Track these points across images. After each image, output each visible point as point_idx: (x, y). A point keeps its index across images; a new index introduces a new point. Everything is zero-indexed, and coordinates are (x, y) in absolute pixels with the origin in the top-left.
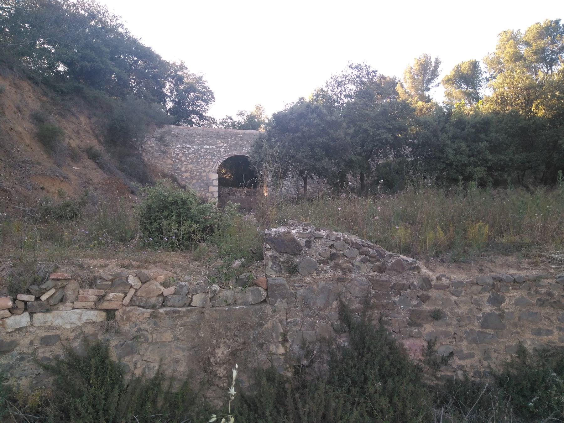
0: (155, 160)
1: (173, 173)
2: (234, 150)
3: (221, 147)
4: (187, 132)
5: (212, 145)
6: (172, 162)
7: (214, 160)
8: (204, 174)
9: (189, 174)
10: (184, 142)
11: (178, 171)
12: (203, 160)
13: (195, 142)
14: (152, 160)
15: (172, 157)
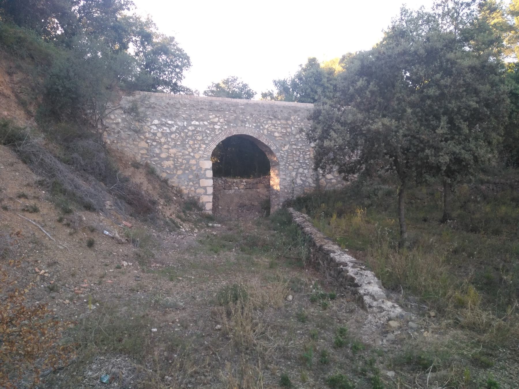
0: (122, 142)
1: (149, 162)
2: (233, 127)
3: (215, 123)
4: (168, 101)
5: (203, 121)
6: (146, 145)
7: (207, 142)
8: (193, 162)
9: (172, 162)
10: (163, 115)
11: (156, 159)
12: (191, 142)
13: (179, 116)
14: (117, 143)
15: (147, 139)
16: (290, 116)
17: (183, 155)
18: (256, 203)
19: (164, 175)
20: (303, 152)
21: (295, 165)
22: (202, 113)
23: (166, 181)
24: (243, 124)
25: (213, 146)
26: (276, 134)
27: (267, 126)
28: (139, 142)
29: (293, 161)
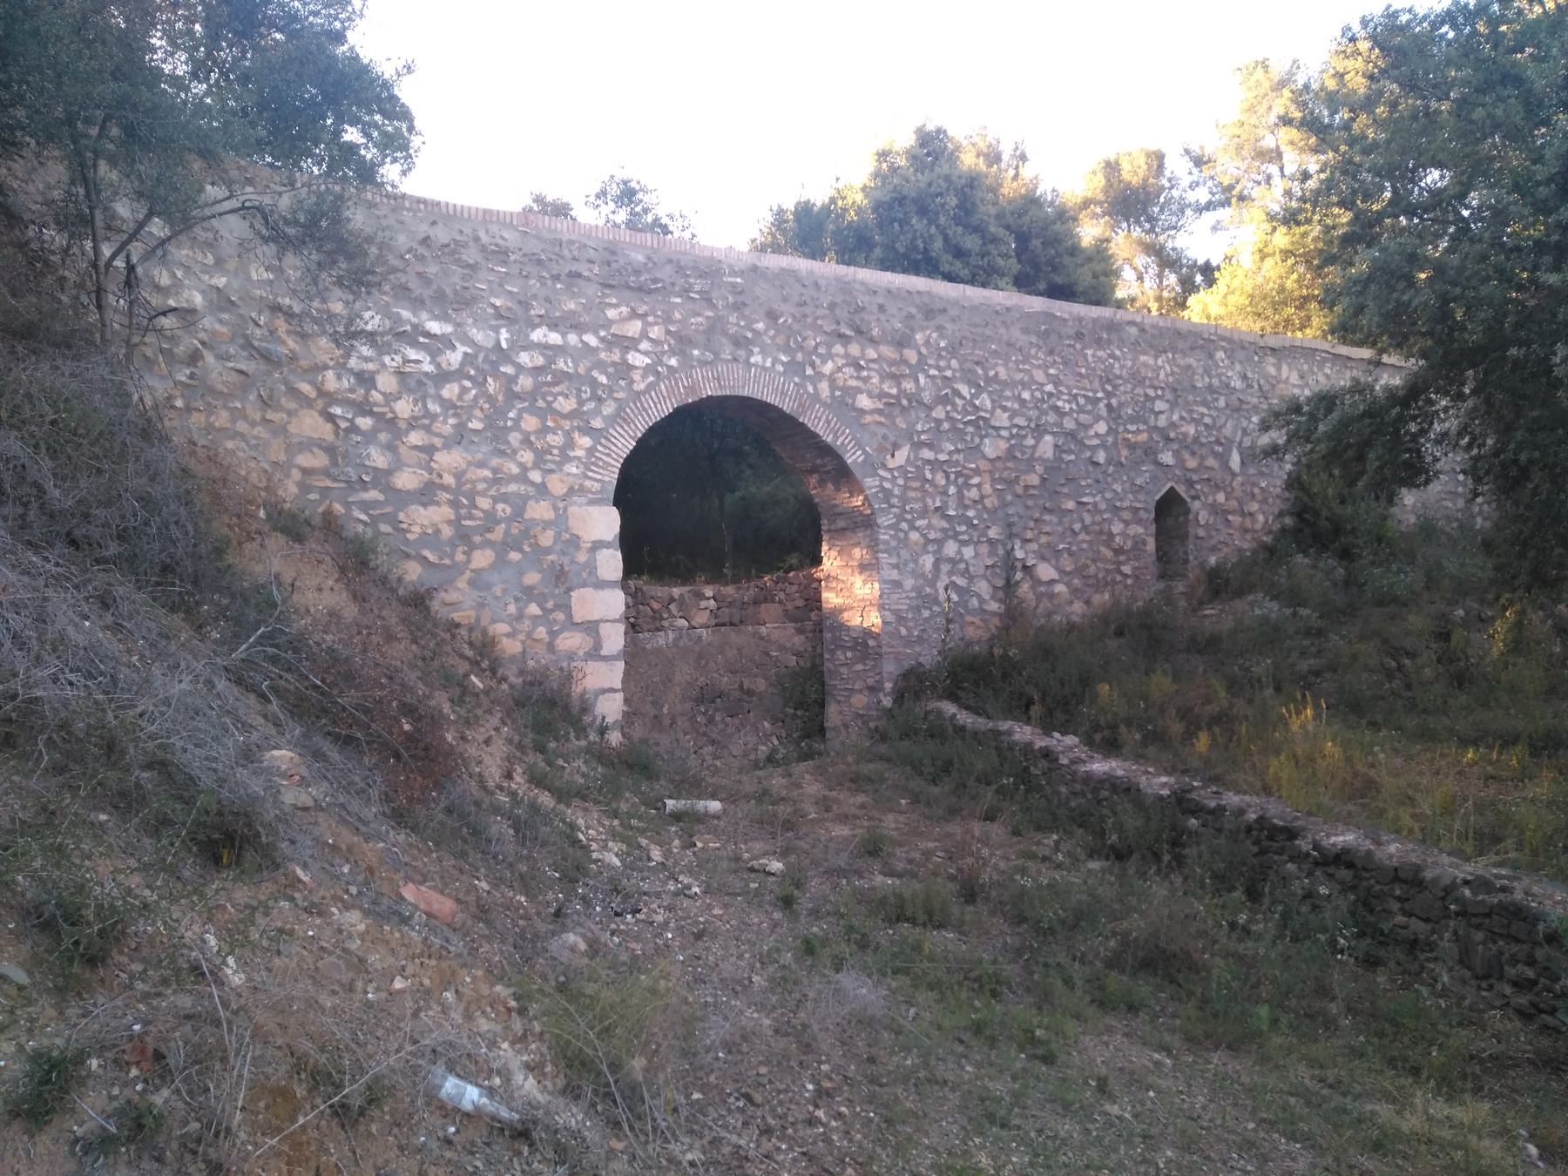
0: (210, 409)
1: (338, 508)
2: (703, 363)
3: (629, 344)
4: (423, 229)
5: (579, 328)
6: (326, 431)
7: (597, 423)
8: (539, 510)
9: (447, 512)
10: (403, 291)
11: (373, 495)
12: (530, 423)
13: (475, 299)
14: (189, 409)
15: (329, 397)
16: (913, 330)
17: (496, 481)
18: (761, 685)
19: (413, 572)
20: (958, 474)
21: (930, 526)
22: (574, 296)
23: (419, 601)
24: (742, 353)
25: (625, 445)
26: (864, 402)
27: (828, 368)
28: (290, 413)
29: (924, 513)
